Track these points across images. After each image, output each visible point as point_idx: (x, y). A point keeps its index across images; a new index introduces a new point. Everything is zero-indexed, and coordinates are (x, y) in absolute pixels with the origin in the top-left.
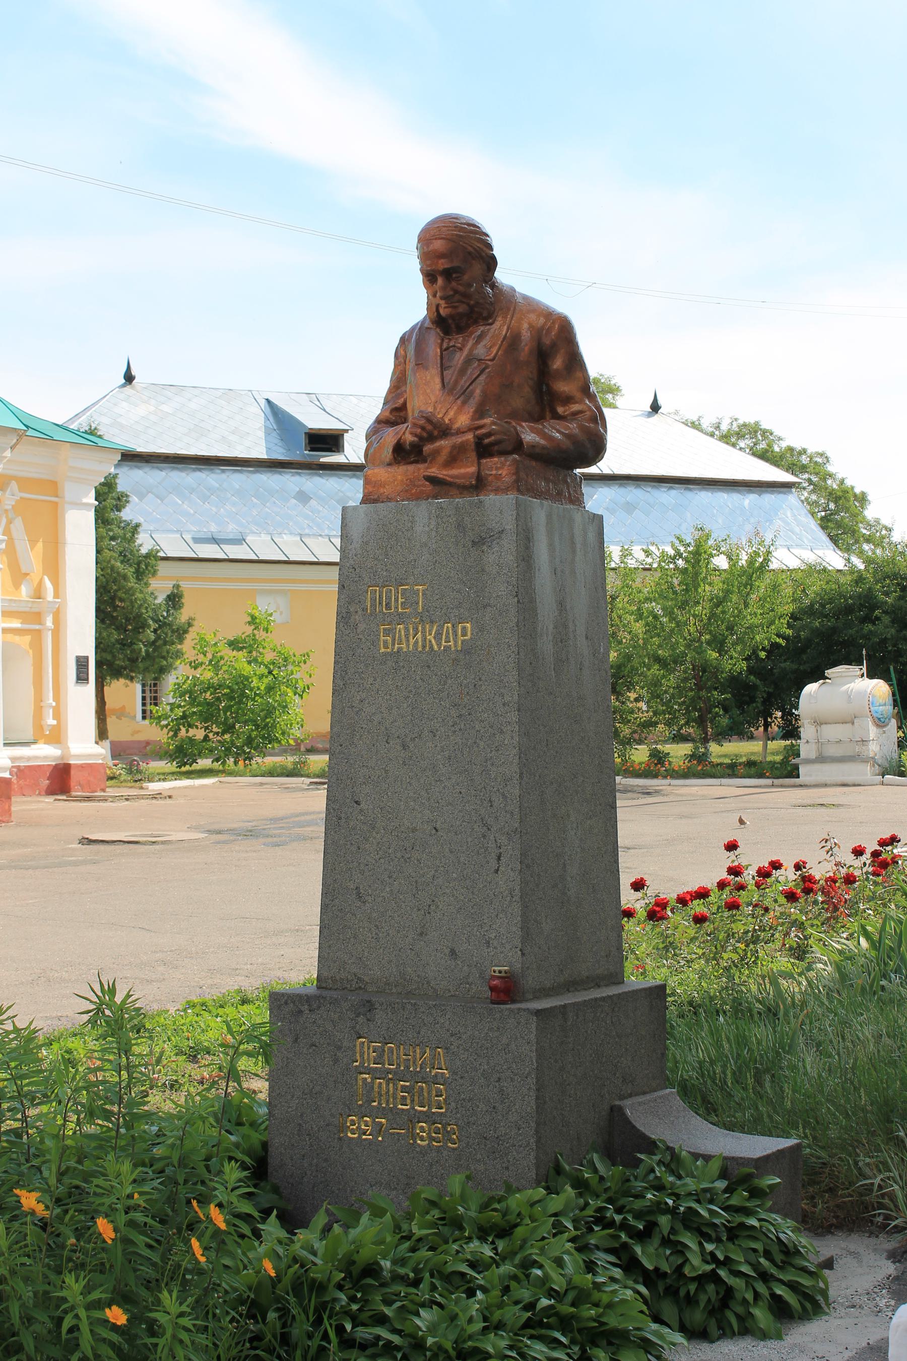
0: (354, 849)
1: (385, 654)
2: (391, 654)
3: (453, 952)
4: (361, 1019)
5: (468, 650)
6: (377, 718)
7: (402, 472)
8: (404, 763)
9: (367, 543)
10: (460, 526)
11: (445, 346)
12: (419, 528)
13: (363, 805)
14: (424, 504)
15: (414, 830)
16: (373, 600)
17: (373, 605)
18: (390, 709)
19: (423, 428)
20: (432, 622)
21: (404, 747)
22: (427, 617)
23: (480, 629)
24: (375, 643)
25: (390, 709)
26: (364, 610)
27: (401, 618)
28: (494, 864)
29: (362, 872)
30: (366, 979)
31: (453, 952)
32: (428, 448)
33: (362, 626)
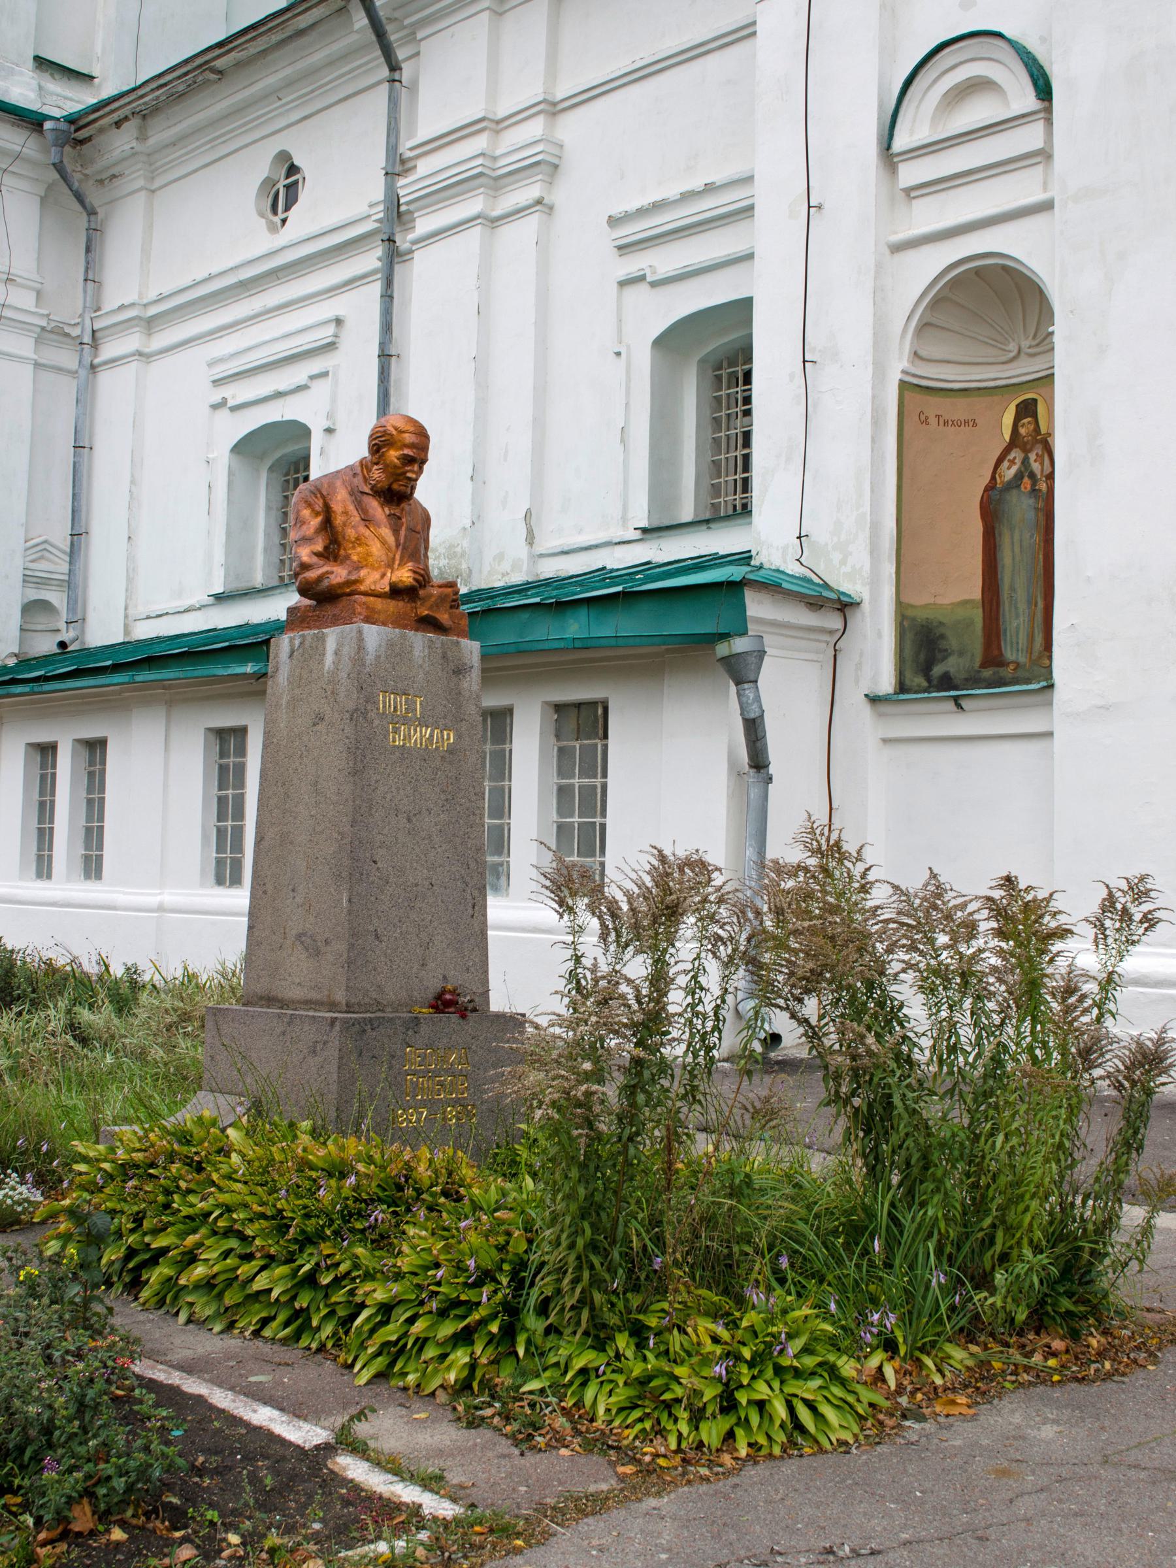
0: (373, 899)
1: (395, 746)
2: (398, 747)
3: (445, 977)
4: (410, 1033)
5: (451, 751)
6: (389, 796)
7: (392, 606)
8: (409, 833)
9: (379, 657)
10: (444, 656)
11: (387, 511)
12: (417, 653)
13: (379, 864)
14: (420, 634)
15: (417, 885)
16: (384, 702)
17: (384, 707)
18: (398, 789)
19: (422, 576)
20: (427, 727)
21: (409, 820)
22: (423, 723)
23: (459, 736)
24: (386, 737)
25: (398, 789)
26: (378, 709)
27: (405, 721)
28: (470, 911)
29: (379, 918)
30: (385, 1002)
31: (445, 977)
32: (421, 592)
33: (376, 722)
